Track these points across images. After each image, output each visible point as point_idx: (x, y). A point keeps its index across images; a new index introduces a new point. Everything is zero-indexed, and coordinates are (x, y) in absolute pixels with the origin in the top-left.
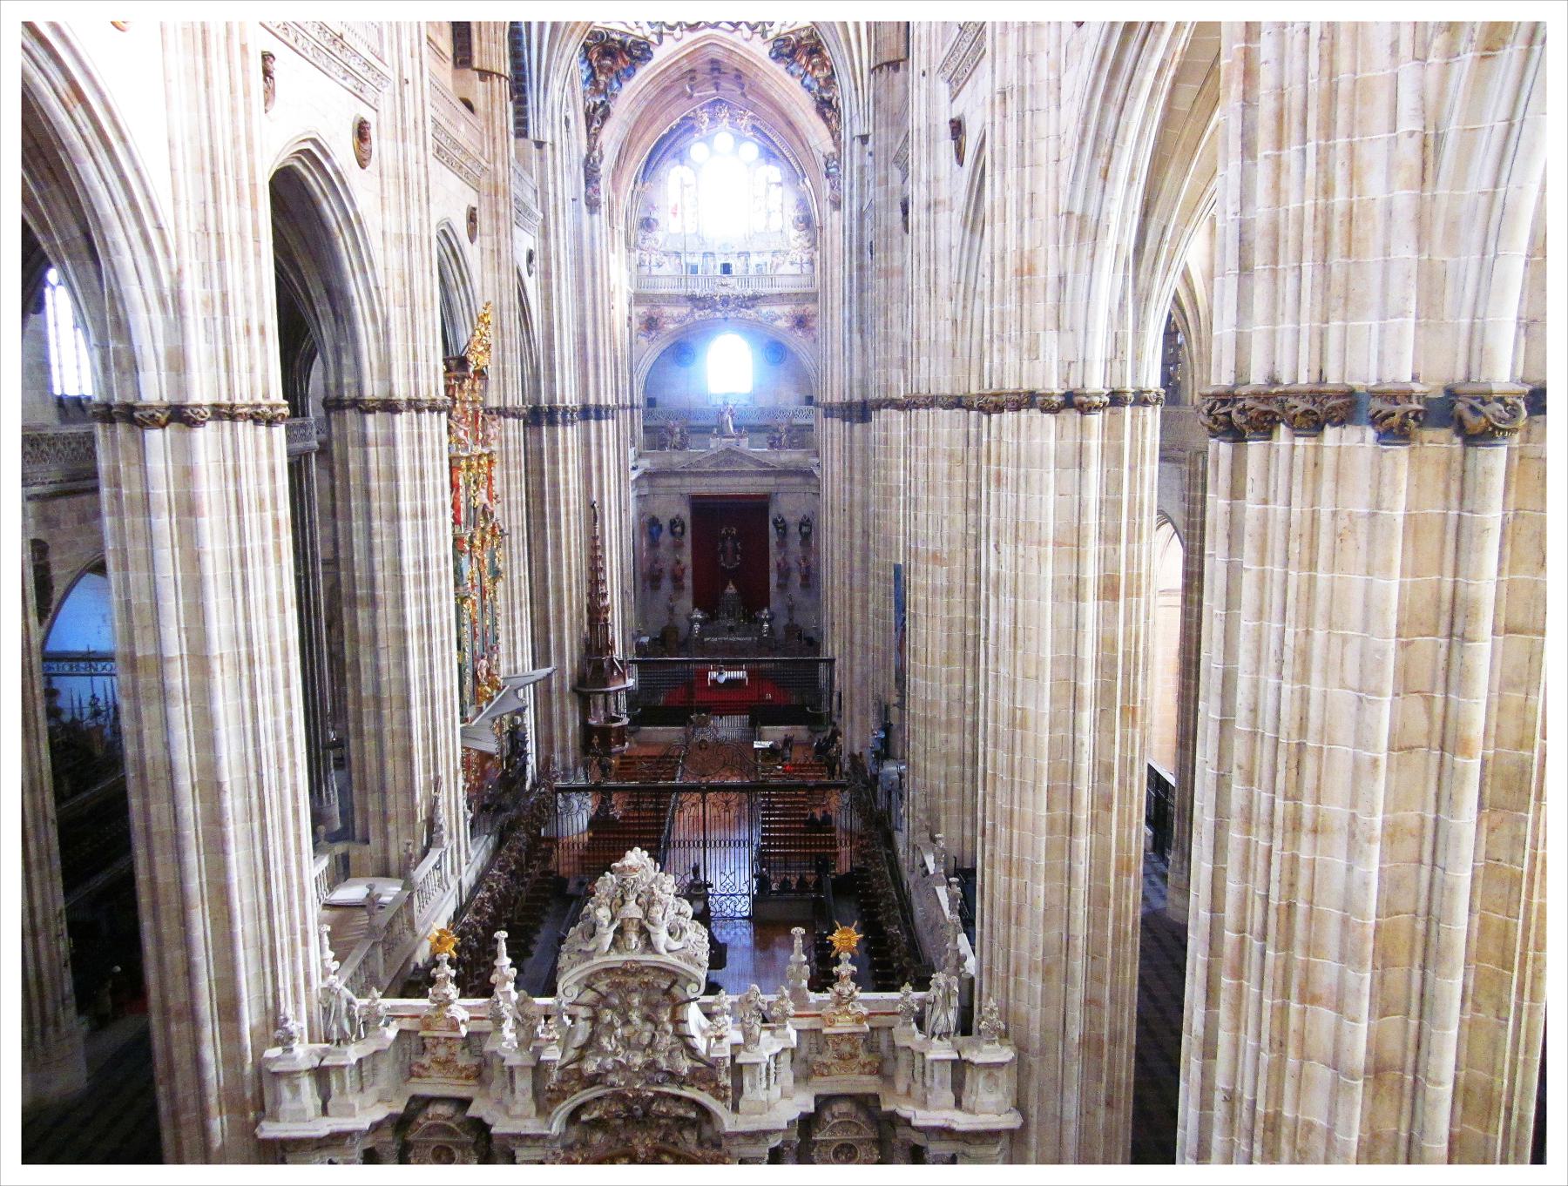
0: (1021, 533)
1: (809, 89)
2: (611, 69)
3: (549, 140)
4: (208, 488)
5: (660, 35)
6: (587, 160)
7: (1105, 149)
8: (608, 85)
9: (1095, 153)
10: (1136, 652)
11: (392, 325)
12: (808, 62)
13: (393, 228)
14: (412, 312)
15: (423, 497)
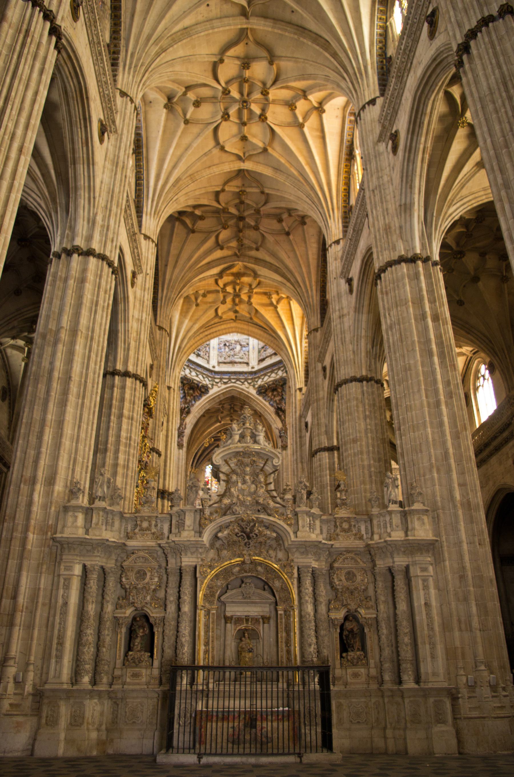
0: (398, 303)
1: (272, 405)
2: (192, 395)
3: (172, 386)
4: (90, 276)
5: (213, 385)
6: (179, 428)
7: (410, 178)
8: (190, 401)
9: (407, 182)
10: (451, 344)
11: (131, 346)
12: (272, 395)
13: (136, 316)
14: (139, 345)
15: (133, 412)
